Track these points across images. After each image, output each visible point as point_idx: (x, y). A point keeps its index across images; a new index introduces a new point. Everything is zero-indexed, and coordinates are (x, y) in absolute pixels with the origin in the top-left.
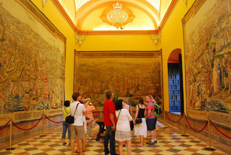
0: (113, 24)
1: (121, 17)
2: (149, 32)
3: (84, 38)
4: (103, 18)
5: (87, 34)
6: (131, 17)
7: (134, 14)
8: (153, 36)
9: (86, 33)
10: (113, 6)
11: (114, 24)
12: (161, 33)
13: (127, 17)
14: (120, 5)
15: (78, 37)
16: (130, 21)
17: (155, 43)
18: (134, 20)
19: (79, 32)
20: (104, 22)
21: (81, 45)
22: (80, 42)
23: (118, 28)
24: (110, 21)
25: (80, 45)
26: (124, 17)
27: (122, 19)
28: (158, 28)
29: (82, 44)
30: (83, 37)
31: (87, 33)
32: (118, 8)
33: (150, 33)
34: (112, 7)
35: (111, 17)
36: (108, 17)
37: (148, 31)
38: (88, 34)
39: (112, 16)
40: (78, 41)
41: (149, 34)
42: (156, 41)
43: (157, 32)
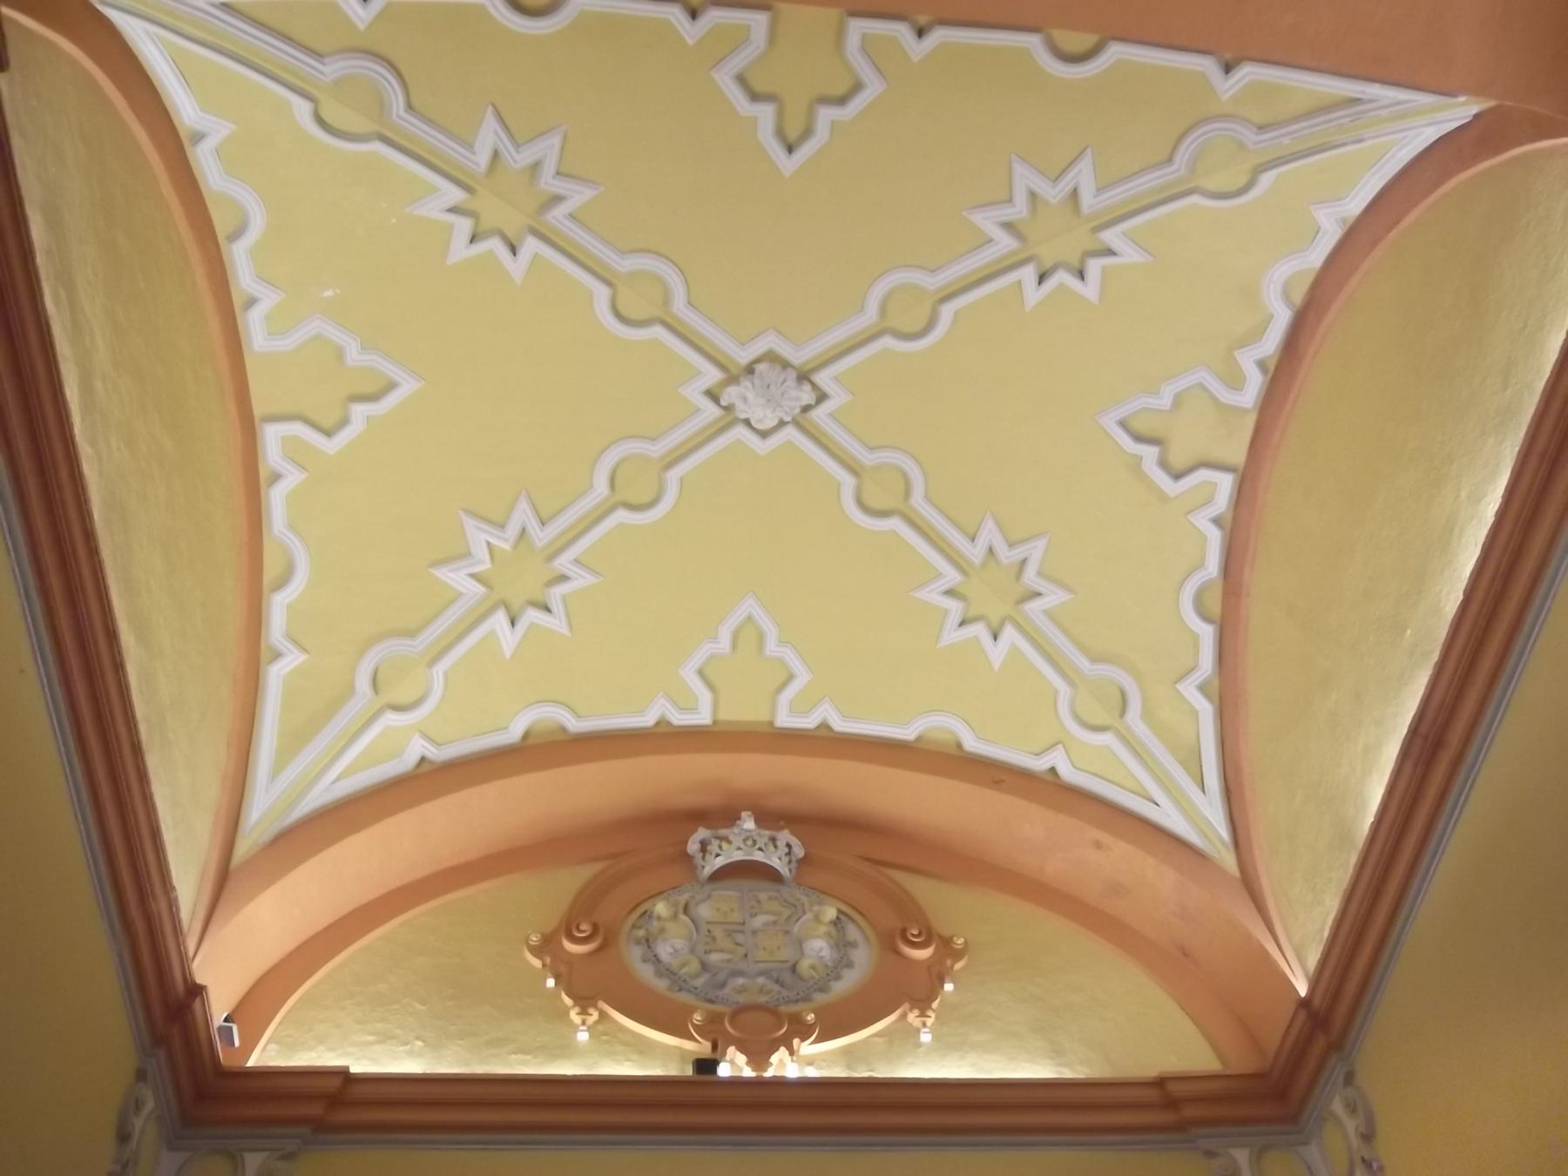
0: (697, 1017)
1: (786, 954)
7: (942, 926)
9: (315, 1110)
10: (693, 847)
11: (714, 1020)
12: (1349, 1079)
13: (864, 958)
16: (902, 989)
18: (949, 987)
20: (584, 1002)
23: (758, 1057)
26: (819, 948)
27: (804, 965)
32: (758, 856)
33: (1190, 1112)
34: (687, 858)
35: (664, 951)
36: (634, 956)
39: (680, 943)
41: (1181, 1127)
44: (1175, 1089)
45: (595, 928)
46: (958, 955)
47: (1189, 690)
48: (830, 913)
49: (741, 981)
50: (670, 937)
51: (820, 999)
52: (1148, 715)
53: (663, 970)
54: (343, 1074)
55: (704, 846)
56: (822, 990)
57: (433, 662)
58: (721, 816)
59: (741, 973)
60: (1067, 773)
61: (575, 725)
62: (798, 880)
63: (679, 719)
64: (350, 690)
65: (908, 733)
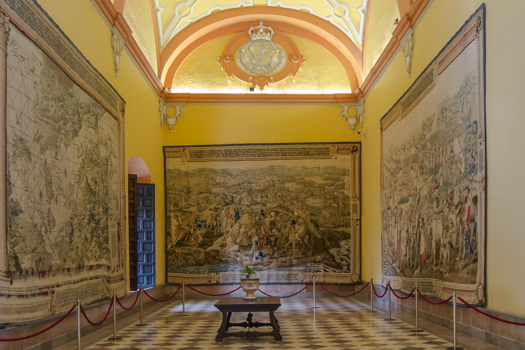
2: (336, 99)
3: (180, 112)
4: (226, 64)
5: (187, 102)
6: (295, 60)
7: (302, 53)
8: (346, 108)
9: (186, 100)
11: (254, 77)
12: (364, 102)
13: (284, 60)
14: (267, 31)
15: (165, 107)
16: (290, 70)
17: (349, 125)
18: (300, 69)
19: (167, 98)
20: (229, 74)
21: (173, 129)
22: (171, 121)
23: (262, 88)
24: (243, 69)
25: (170, 126)
26: (275, 59)
27: (272, 64)
28: (357, 91)
29: (174, 125)
30: (178, 108)
31: (188, 98)
32: (263, 38)
33: (339, 100)
36: (237, 60)
37: (334, 95)
38: (190, 100)
39: (247, 59)
40: (166, 118)
41: (336, 102)
42: (352, 121)
43: (356, 98)
44: (336, 96)
45: (230, 56)
46: (304, 61)
47: (360, 11)
48: (278, 51)
49: (259, 68)
50: (245, 57)
51: (275, 72)
52: (350, 15)
53: (244, 65)
54: (190, 94)
55: (252, 32)
56: (276, 69)
57: (190, 7)
58: (255, 23)
59: (258, 66)
60: (332, 22)
61: (222, 9)
62: (272, 40)
63: (245, 5)
64: (174, 15)
65: (298, 9)
